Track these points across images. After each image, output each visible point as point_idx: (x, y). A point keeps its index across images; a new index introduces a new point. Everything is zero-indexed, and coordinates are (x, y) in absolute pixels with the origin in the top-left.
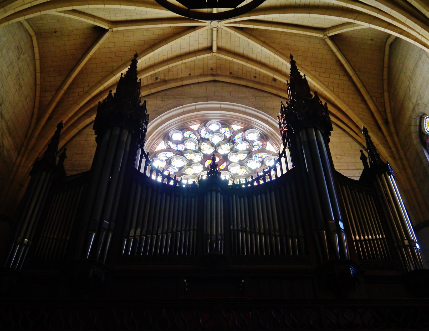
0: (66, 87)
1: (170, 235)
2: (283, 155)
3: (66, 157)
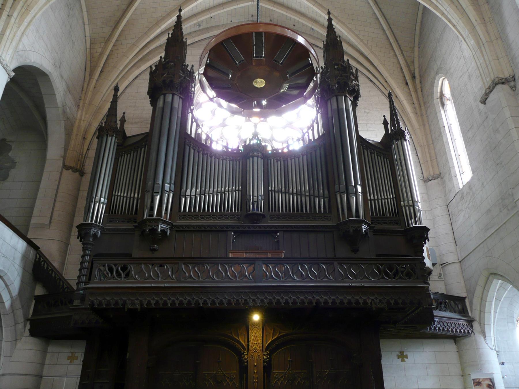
0: (114, 40)
1: (220, 195)
3: (125, 121)
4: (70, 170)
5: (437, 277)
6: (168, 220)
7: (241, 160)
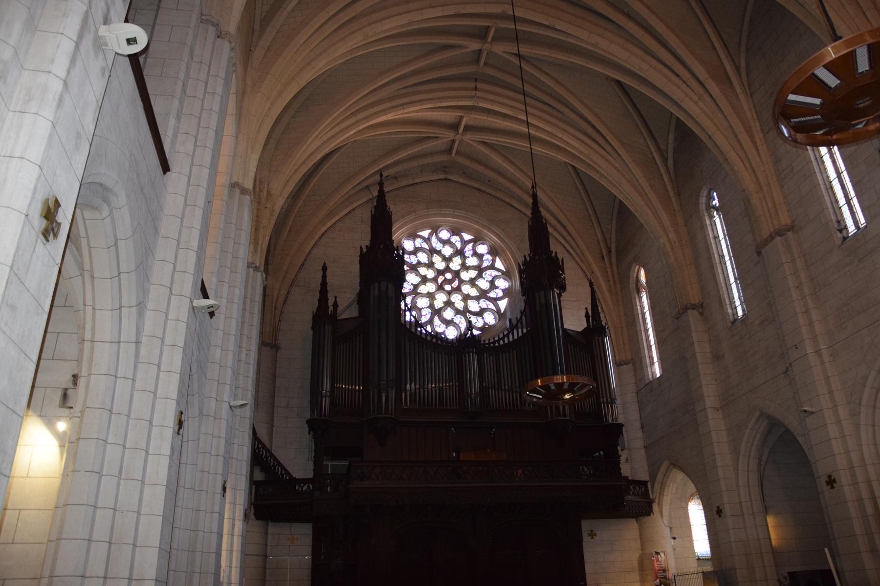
2: (524, 313)
4: (268, 347)
5: (624, 461)
6: (393, 417)
7: (456, 354)
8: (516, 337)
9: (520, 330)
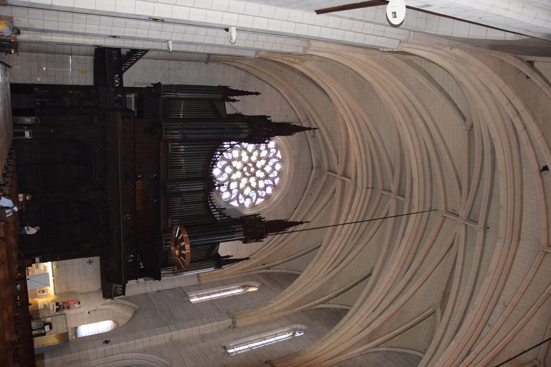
4: (207, 57)
8: (214, 213)
9: (218, 216)
